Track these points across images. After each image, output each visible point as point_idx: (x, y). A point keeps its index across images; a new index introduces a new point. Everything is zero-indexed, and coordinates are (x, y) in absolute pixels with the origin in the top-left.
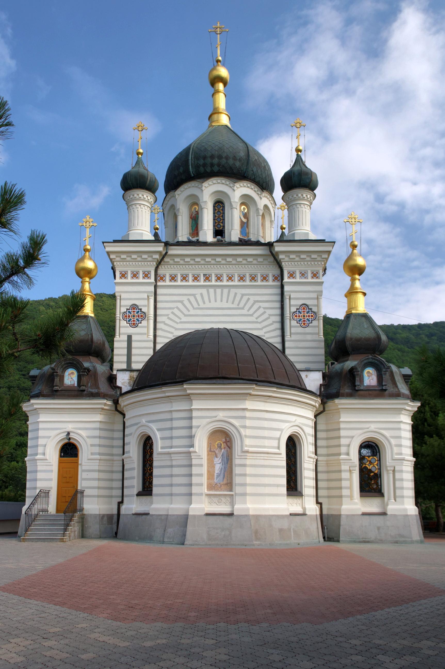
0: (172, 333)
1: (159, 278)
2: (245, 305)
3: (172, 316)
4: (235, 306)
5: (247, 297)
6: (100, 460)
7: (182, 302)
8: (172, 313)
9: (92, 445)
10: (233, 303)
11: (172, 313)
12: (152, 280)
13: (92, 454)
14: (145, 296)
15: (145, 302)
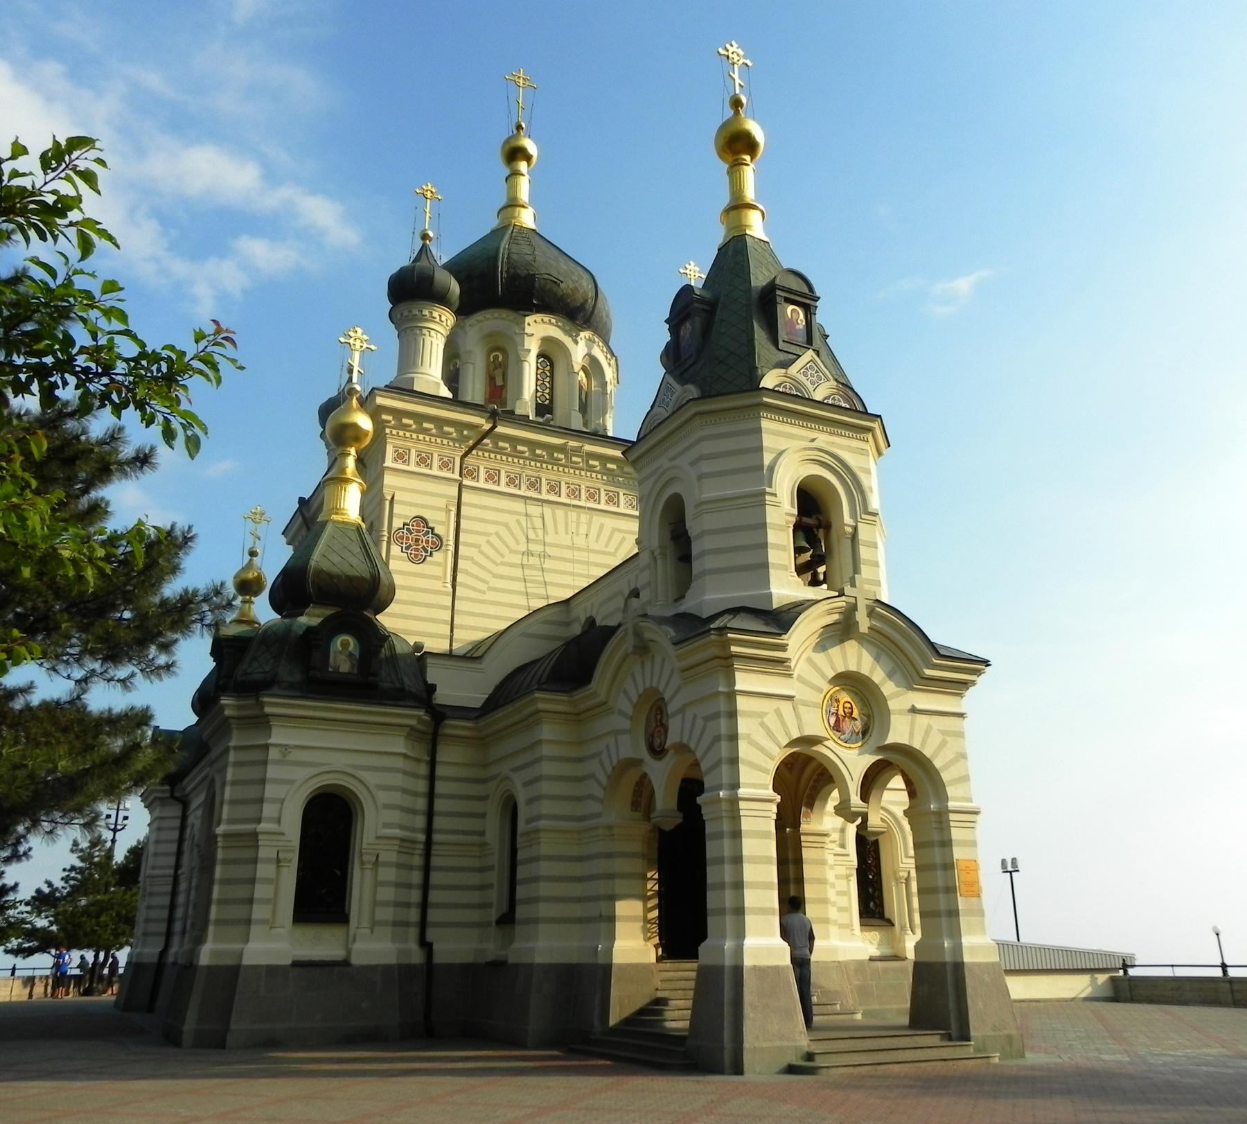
0: (487, 582)
1: (465, 472)
2: (617, 549)
3: (486, 548)
4: (600, 546)
5: (621, 535)
6: (402, 840)
7: (506, 525)
8: (488, 542)
9: (386, 806)
10: (597, 541)
11: (488, 542)
12: (456, 476)
13: (386, 825)
14: (442, 503)
15: (441, 516)
